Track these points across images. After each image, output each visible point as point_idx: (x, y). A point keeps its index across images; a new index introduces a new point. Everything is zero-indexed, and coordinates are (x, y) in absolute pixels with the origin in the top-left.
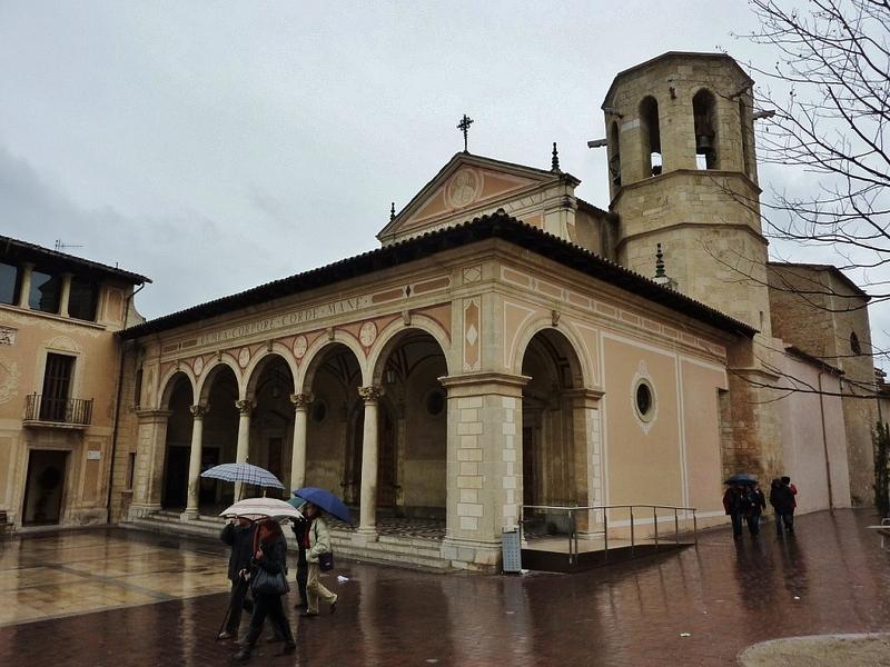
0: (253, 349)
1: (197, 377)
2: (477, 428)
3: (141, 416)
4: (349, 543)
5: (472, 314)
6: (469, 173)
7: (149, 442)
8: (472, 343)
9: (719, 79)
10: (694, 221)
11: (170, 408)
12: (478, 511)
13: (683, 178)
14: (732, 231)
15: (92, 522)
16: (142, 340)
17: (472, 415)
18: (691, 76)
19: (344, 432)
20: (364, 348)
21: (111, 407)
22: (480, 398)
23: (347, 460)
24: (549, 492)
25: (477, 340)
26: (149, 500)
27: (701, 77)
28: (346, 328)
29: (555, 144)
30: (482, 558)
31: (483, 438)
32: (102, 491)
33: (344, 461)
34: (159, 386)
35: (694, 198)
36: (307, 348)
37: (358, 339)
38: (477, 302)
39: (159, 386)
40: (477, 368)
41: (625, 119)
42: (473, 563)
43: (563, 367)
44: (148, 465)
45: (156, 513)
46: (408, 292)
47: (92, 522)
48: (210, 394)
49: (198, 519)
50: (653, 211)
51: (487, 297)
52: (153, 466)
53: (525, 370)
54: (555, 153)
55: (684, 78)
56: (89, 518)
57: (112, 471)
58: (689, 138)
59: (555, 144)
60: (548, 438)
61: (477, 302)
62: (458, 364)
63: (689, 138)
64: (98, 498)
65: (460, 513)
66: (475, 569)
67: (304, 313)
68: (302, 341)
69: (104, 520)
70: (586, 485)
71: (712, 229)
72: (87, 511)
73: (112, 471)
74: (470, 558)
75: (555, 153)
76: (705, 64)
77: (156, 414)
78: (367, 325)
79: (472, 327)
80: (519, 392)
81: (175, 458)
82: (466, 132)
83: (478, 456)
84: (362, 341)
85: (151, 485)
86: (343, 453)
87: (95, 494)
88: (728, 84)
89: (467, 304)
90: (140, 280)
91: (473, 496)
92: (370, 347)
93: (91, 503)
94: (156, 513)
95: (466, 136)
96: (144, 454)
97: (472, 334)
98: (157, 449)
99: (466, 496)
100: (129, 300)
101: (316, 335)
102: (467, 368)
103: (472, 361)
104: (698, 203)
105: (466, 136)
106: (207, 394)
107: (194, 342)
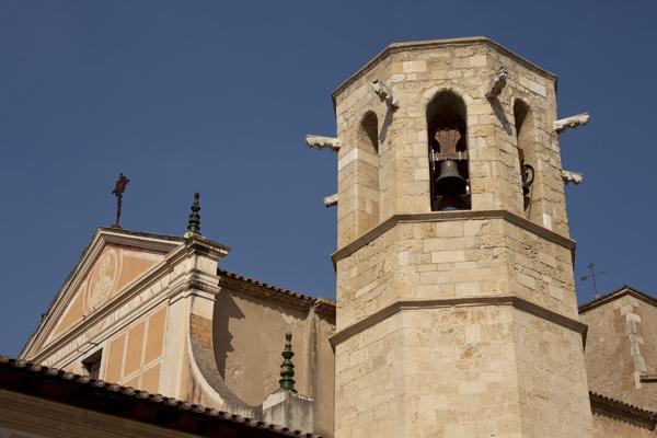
9: (468, 74)
10: (420, 296)
13: (403, 228)
14: (490, 309)
18: (423, 73)
27: (439, 74)
29: (197, 196)
35: (422, 261)
41: (341, 152)
50: (366, 289)
54: (196, 209)
55: (414, 77)
58: (418, 166)
59: (197, 196)
63: (418, 166)
71: (453, 309)
75: (196, 209)
76: (447, 55)
95: (120, 202)
104: (429, 267)
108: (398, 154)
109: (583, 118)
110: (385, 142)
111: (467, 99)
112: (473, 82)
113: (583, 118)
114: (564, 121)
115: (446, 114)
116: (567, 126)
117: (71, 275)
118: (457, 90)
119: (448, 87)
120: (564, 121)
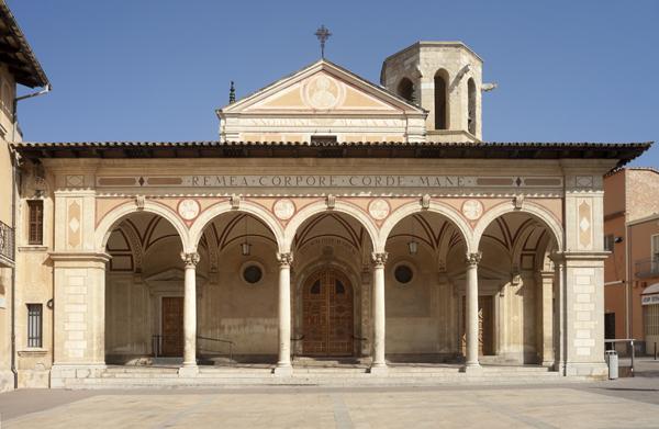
6: (331, 82)
8: (585, 229)
24: (509, 339)
25: (589, 229)
26: (95, 358)
34: (97, 225)
36: (390, 213)
39: (97, 225)
42: (591, 376)
43: (535, 250)
53: (108, 249)
60: (509, 303)
65: (576, 345)
74: (589, 373)
77: (96, 258)
80: (103, 265)
82: (323, 42)
83: (84, 327)
84: (466, 214)
95: (323, 46)
99: (580, 334)
102: (581, 248)
105: (323, 46)
107: (178, 181)
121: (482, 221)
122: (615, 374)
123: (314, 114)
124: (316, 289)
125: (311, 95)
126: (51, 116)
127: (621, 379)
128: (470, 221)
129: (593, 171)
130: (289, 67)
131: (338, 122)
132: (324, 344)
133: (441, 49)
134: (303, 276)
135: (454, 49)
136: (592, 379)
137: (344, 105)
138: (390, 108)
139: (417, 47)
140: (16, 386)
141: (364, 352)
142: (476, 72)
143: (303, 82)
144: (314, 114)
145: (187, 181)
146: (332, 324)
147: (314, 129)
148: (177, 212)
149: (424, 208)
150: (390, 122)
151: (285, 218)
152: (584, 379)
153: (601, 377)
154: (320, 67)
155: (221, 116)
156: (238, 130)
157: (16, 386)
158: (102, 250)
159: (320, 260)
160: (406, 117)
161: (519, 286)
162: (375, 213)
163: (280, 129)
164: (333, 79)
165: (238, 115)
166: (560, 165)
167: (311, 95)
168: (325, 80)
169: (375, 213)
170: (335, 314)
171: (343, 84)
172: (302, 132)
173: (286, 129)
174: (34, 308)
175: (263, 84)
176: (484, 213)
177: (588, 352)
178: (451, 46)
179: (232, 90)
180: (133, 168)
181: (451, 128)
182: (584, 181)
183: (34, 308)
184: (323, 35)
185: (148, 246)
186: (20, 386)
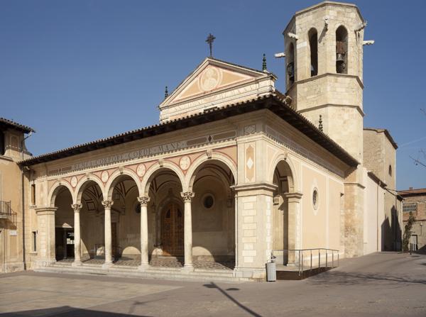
0: (110, 172)
1: (74, 188)
2: (253, 213)
3: (38, 211)
4: (179, 273)
5: (250, 152)
7: (45, 227)
11: (55, 205)
12: (254, 253)
15: (16, 270)
16: (34, 167)
17: (251, 206)
19: (154, 219)
20: (183, 171)
21: (19, 206)
22: (255, 197)
23: (157, 231)
28: (170, 159)
30: (257, 275)
31: (254, 217)
32: (19, 253)
33: (155, 234)
34: (48, 193)
37: (179, 166)
38: (252, 145)
39: (48, 193)
40: (253, 181)
44: (47, 238)
45: (54, 263)
46: (210, 139)
47: (16, 270)
48: (82, 197)
49: (82, 265)
51: (260, 142)
52: (49, 239)
56: (14, 268)
57: (24, 242)
61: (252, 145)
62: (241, 179)
64: (18, 256)
66: (253, 281)
67: (143, 151)
68: (142, 167)
69: (22, 269)
70: (294, 240)
72: (13, 264)
73: (24, 242)
77: (49, 209)
78: (184, 158)
79: (250, 159)
81: (62, 236)
82: (211, 44)
84: (181, 166)
85: (49, 249)
86: (155, 230)
87: (16, 255)
88: (354, 23)
89: (247, 146)
90: (27, 131)
91: (251, 246)
92: (187, 170)
93: (14, 260)
94: (54, 263)
96: (43, 231)
97: (250, 163)
98: (51, 229)
99: (246, 247)
100: (22, 143)
101: (152, 163)
103: (250, 177)
106: (80, 198)
108: (328, 49)
109: (372, 42)
110: (322, 43)
111: (348, 30)
112: (351, 24)
113: (372, 42)
114: (366, 42)
115: (341, 34)
116: (367, 44)
117: (191, 74)
118: (346, 26)
119: (343, 24)
120: (366, 42)
121: (189, 170)
122: (273, 276)
123: (205, 95)
124: (168, 216)
125: (203, 83)
126: (37, 146)
127: (278, 282)
128: (183, 171)
129: (254, 121)
130: (189, 71)
131: (218, 96)
132: (172, 249)
133: (311, 12)
134: (161, 208)
135: (320, 9)
136: (253, 281)
137: (221, 84)
138: (249, 77)
139: (293, 20)
140: (25, 269)
141: (158, 251)
142: (351, 20)
143: (199, 76)
144: (205, 95)
145: (73, 166)
146: (176, 236)
147: (203, 106)
148: (179, 166)
149: (161, 166)
150: (248, 88)
151: (105, 178)
152: (247, 280)
153: (259, 280)
154: (208, 63)
155: (161, 109)
156: (169, 115)
157: (25, 269)
158: (53, 206)
159: (168, 197)
160: (257, 82)
161: (279, 205)
162: (140, 173)
163: (187, 110)
164: (214, 68)
165: (168, 107)
166: (229, 122)
167: (203, 83)
168: (211, 69)
169: (140, 173)
170: (177, 231)
171: (221, 69)
172: (198, 108)
173: (190, 109)
174: (35, 233)
175: (179, 83)
176: (191, 164)
177: (251, 260)
178: (318, 7)
179: (264, 60)
180: (54, 165)
181: (318, 74)
182: (251, 128)
183: (35, 233)
184: (210, 39)
185: (126, 194)
186: (28, 269)
